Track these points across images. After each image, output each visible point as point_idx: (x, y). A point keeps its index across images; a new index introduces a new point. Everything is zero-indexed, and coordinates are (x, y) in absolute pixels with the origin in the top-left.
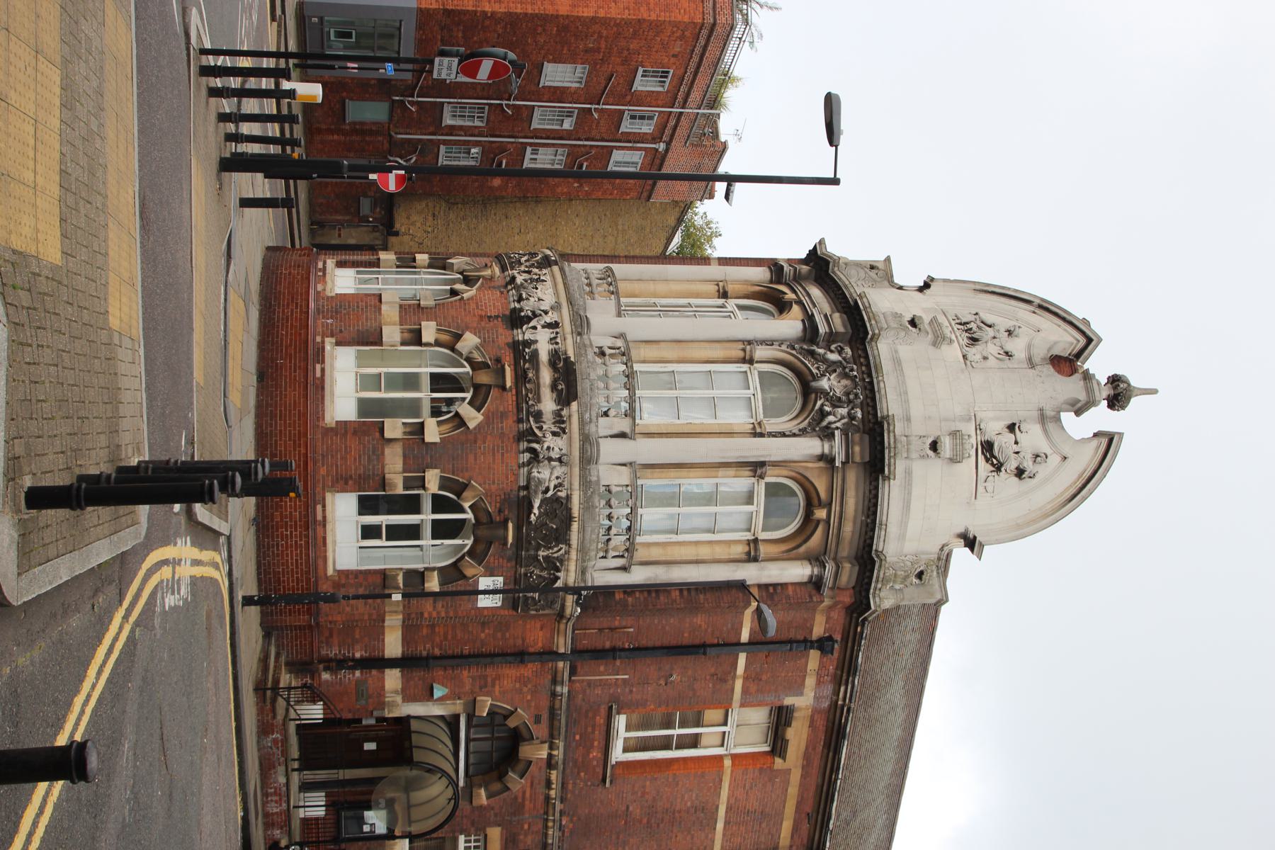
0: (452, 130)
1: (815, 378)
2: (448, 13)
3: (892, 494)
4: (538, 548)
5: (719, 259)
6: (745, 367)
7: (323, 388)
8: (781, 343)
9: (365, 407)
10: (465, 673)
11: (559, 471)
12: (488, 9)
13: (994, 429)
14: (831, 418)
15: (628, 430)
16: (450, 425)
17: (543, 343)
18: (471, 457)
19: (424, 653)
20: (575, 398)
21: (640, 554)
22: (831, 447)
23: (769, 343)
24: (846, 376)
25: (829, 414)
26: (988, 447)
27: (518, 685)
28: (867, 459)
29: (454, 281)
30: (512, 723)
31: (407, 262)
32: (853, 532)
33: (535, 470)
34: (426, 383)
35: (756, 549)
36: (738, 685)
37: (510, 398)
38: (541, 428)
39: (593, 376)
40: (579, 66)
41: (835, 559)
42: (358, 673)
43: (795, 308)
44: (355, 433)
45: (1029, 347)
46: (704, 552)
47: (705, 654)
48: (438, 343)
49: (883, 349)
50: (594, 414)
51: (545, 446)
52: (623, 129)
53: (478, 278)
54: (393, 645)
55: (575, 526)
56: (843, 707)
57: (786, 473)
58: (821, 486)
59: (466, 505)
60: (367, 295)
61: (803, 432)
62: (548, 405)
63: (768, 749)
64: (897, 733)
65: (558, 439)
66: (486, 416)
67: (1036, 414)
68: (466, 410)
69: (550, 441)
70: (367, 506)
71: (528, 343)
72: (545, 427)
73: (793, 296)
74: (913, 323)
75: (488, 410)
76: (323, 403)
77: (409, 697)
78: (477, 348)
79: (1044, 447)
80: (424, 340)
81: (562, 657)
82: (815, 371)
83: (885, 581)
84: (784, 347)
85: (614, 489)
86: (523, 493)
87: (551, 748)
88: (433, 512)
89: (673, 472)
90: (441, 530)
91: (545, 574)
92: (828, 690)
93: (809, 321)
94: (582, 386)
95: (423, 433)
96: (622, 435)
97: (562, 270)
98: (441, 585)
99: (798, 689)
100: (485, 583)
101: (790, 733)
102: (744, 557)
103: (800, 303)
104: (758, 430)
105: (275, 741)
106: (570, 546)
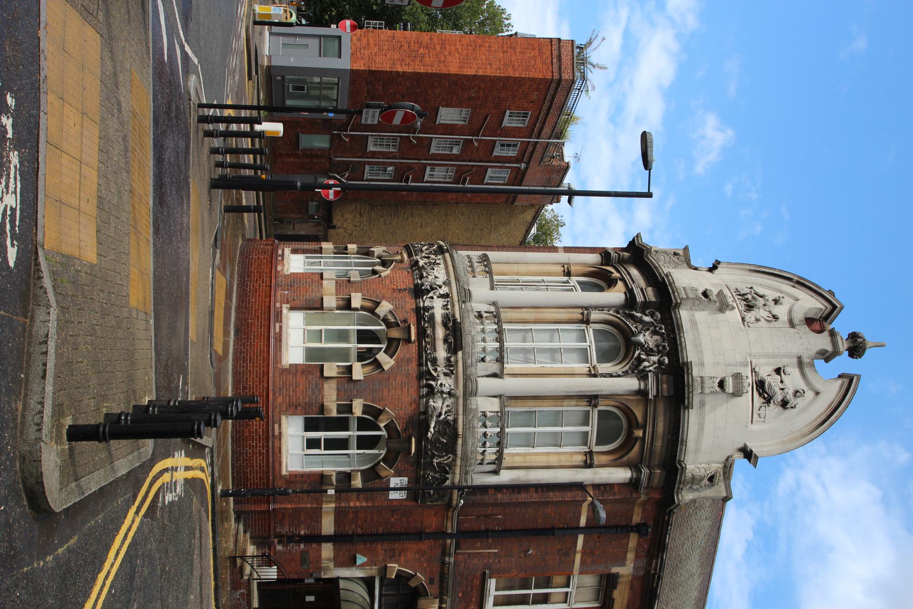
0: (374, 154)
1: (633, 334)
2: (372, 73)
3: (692, 418)
4: (433, 456)
5: (565, 248)
6: (583, 327)
7: (281, 340)
8: (609, 307)
9: (311, 353)
10: (380, 546)
11: (449, 401)
12: (400, 70)
13: (765, 372)
14: (646, 364)
15: (498, 372)
16: (371, 367)
18: (386, 391)
19: (350, 532)
20: (461, 349)
21: (507, 461)
22: (646, 385)
23: (600, 308)
24: (655, 333)
25: (644, 360)
26: (760, 385)
27: (417, 556)
28: (672, 393)
29: (374, 264)
30: (413, 584)
31: (342, 251)
32: (662, 446)
33: (431, 400)
34: (354, 337)
35: (592, 459)
36: (578, 557)
37: (414, 348)
38: (436, 370)
39: (474, 333)
40: (464, 109)
41: (649, 467)
42: (302, 546)
43: (620, 284)
44: (303, 372)
45: (790, 312)
46: (553, 460)
47: (553, 535)
48: (363, 308)
49: (684, 314)
50: (474, 360)
51: (439, 382)
52: (495, 153)
53: (392, 261)
54: (328, 526)
55: (460, 441)
56: (654, 574)
57: (613, 403)
58: (639, 413)
59: (382, 425)
60: (313, 274)
61: (626, 374)
62: (441, 353)
63: (596, 605)
64: (695, 594)
65: (448, 378)
66: (397, 361)
67: (795, 360)
68: (382, 357)
69: (443, 380)
70: (310, 426)
71: (427, 309)
72: (439, 369)
73: (618, 275)
74: (705, 294)
75: (398, 357)
76: (280, 351)
77: (340, 562)
78: (390, 311)
79: (801, 385)
80: (354, 305)
81: (451, 536)
82: (634, 329)
83: (685, 483)
84: (611, 312)
85: (489, 414)
86: (422, 417)
87: (441, 602)
88: (358, 430)
89: (531, 403)
90: (363, 443)
91: (437, 475)
92: (643, 563)
93: (630, 292)
94: (467, 340)
95: (351, 373)
96: (495, 375)
97: (452, 256)
98: (364, 481)
99: (622, 562)
100: (394, 482)
101: (616, 594)
102: (582, 463)
103: (623, 280)
104: (593, 372)
105: (242, 595)
106: (456, 455)
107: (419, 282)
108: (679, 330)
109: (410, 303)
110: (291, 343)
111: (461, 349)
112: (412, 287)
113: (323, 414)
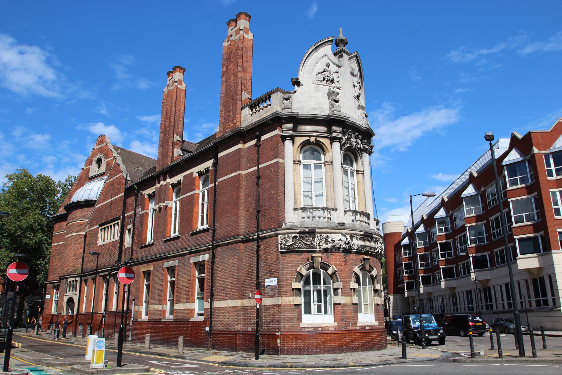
17: (357, 243)
82: (348, 145)
109: (352, 256)
110: (369, 321)
111: (372, 234)
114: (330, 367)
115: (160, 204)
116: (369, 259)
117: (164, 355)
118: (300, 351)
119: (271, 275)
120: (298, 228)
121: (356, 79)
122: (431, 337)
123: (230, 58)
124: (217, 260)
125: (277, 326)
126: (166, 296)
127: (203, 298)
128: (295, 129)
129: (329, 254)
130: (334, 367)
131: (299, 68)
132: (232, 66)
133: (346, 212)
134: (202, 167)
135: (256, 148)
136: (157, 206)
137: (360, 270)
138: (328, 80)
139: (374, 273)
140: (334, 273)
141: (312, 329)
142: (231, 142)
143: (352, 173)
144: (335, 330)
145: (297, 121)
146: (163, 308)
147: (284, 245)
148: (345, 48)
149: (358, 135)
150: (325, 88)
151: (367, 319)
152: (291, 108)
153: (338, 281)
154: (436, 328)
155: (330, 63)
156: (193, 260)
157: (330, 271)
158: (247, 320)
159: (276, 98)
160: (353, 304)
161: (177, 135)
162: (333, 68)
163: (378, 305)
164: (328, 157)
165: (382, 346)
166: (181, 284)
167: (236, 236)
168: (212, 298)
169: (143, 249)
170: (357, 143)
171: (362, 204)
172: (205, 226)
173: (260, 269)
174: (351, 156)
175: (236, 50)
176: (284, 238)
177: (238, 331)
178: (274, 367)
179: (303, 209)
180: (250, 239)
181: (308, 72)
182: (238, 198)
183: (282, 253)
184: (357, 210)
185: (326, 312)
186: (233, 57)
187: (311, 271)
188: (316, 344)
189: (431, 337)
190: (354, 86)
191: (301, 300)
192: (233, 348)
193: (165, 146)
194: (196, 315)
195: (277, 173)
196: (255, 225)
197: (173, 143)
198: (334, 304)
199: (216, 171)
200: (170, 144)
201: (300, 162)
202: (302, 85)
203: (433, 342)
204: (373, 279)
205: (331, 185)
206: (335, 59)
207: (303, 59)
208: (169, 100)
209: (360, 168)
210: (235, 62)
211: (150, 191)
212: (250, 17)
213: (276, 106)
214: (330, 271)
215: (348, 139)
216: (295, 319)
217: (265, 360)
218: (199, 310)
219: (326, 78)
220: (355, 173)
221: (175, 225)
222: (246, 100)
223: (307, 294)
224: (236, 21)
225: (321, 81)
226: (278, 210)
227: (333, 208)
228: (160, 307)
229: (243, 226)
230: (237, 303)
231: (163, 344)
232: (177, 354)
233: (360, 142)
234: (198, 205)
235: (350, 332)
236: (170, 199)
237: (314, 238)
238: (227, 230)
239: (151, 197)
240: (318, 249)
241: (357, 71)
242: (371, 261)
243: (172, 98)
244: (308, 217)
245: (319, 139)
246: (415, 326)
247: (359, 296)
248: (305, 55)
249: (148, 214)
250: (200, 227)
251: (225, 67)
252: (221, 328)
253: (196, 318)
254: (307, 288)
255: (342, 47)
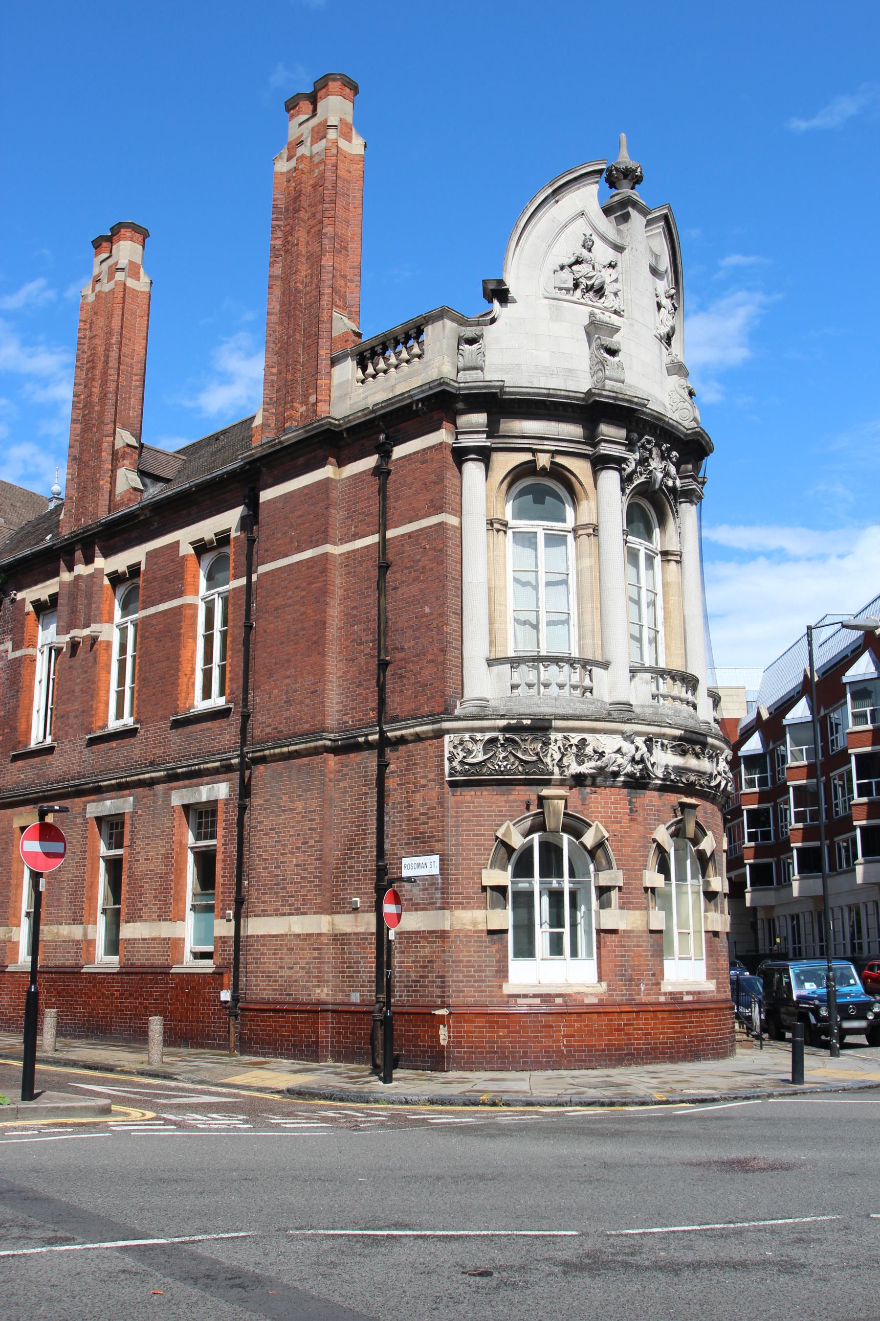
17: (664, 760)
82: (642, 479)
107: (622, 779)
108: (660, 419)
109: (651, 797)
110: (692, 979)
111: (705, 736)
112: (625, 791)
113: (505, 931)
114: (602, 1104)
115: (75, 632)
116: (694, 807)
117: (110, 1069)
118: (503, 1060)
119: (422, 844)
120: (502, 717)
121: (664, 286)
122: (846, 1025)
123: (296, 211)
124: (256, 801)
125: (437, 991)
126: (93, 899)
127: (209, 909)
128: (492, 431)
129: (588, 790)
130: (612, 1104)
131: (506, 249)
132: (301, 235)
133: (633, 672)
134: (207, 528)
135: (375, 482)
136: (67, 638)
137: (672, 836)
138: (589, 289)
139: (707, 844)
140: (600, 845)
141: (538, 1001)
142: (301, 460)
143: (650, 559)
144: (601, 1004)
145: (499, 405)
146: (85, 934)
147: (462, 763)
148: (635, 194)
149: (669, 450)
150: (579, 311)
151: (688, 972)
152: (482, 369)
153: (611, 868)
154: (864, 998)
155: (595, 238)
156: (179, 798)
157: (589, 839)
158: (347, 973)
159: (439, 337)
160: (652, 932)
161: (124, 427)
162: (602, 253)
163: (716, 934)
164: (586, 512)
165: (721, 1049)
166: (141, 867)
167: (317, 733)
168: (241, 909)
169: (20, 763)
170: (667, 474)
171: (678, 651)
172: (217, 701)
173: (388, 829)
174: (649, 508)
175: (314, 186)
176: (462, 742)
177: (319, 1003)
178: (443, 1103)
179: (515, 662)
180: (359, 744)
181: (533, 261)
182: (323, 624)
183: (453, 784)
184: (662, 665)
185: (574, 953)
186: (305, 209)
187: (536, 837)
188: (547, 1042)
189: (846, 1025)
190: (659, 306)
191: (504, 918)
192: (306, 1050)
193: (87, 456)
194: (188, 957)
195: (439, 558)
196: (374, 705)
197: (115, 454)
198: (599, 931)
199: (251, 541)
200: (106, 456)
201: (506, 525)
202: (514, 301)
203: (849, 1039)
204: (703, 861)
205: (594, 593)
206: (606, 225)
207: (516, 225)
208: (101, 322)
209: (673, 547)
210: (312, 222)
211: (42, 591)
212: (355, 89)
213: (437, 360)
214: (589, 839)
215: (643, 462)
216: (489, 972)
217: (407, 1083)
218: (198, 941)
219: (583, 280)
220: (658, 559)
221: (120, 695)
222: (344, 337)
223: (524, 901)
224: (313, 99)
225: (568, 290)
226: (443, 663)
227: (599, 658)
228: (76, 932)
229: (337, 703)
230: (320, 924)
231: (87, 1037)
232: (146, 1067)
233: (673, 470)
234: (195, 638)
235: (642, 1010)
236: (106, 617)
237: (546, 744)
238: (287, 714)
239: (43, 608)
240: (557, 776)
241: (665, 264)
242: (699, 812)
243: (110, 316)
244: (530, 686)
245: (559, 460)
246: (804, 993)
247: (666, 907)
248: (523, 213)
249: (33, 660)
250: (200, 705)
251: (280, 234)
252: (268, 994)
253: (188, 964)
254: (523, 884)
255: (626, 191)
